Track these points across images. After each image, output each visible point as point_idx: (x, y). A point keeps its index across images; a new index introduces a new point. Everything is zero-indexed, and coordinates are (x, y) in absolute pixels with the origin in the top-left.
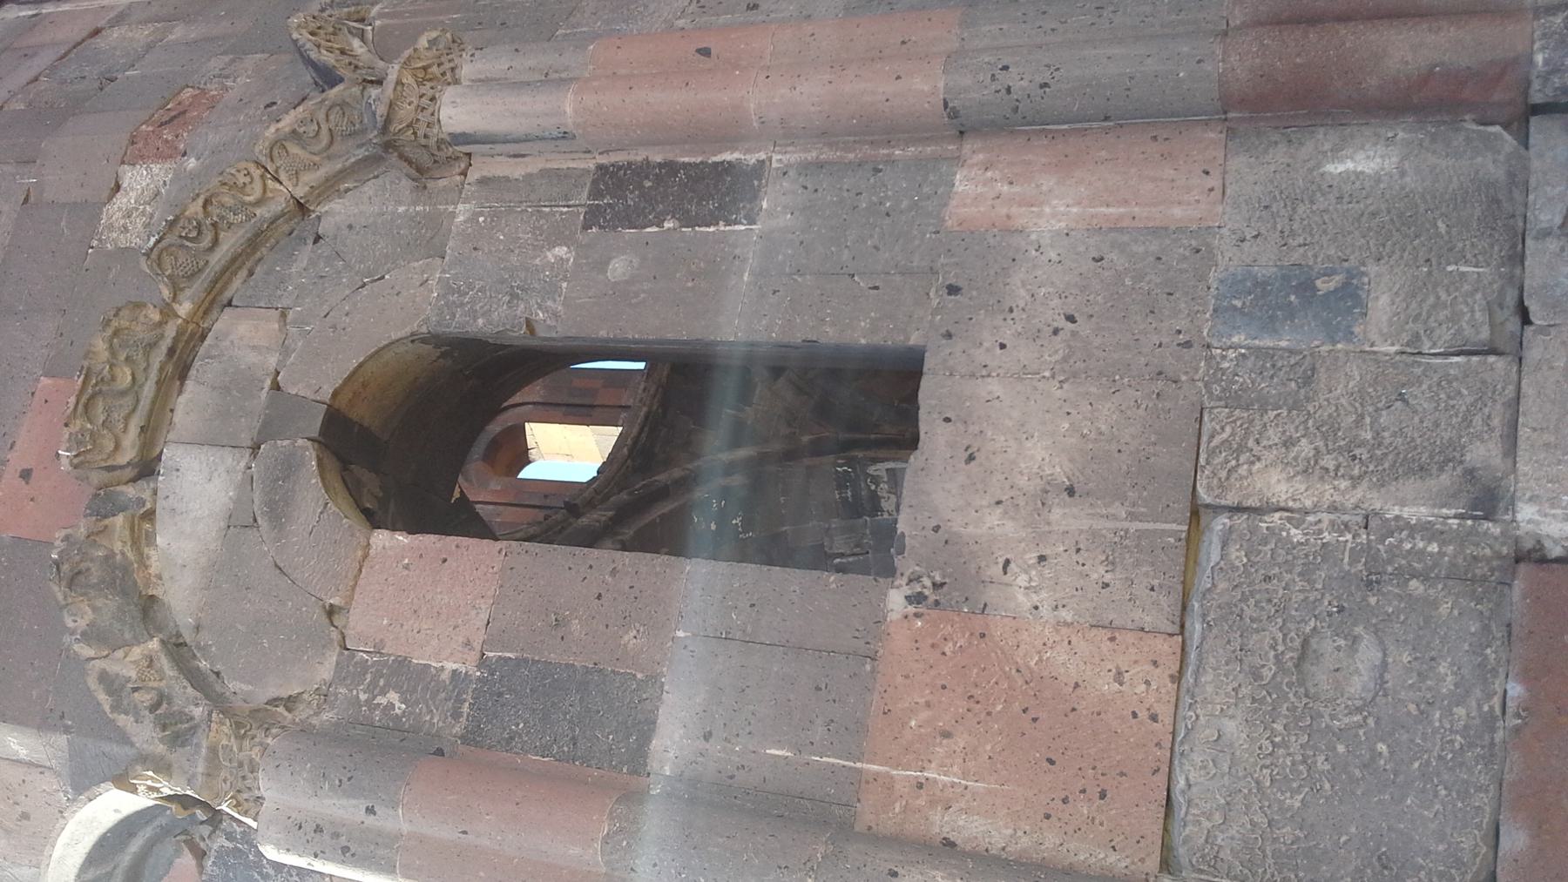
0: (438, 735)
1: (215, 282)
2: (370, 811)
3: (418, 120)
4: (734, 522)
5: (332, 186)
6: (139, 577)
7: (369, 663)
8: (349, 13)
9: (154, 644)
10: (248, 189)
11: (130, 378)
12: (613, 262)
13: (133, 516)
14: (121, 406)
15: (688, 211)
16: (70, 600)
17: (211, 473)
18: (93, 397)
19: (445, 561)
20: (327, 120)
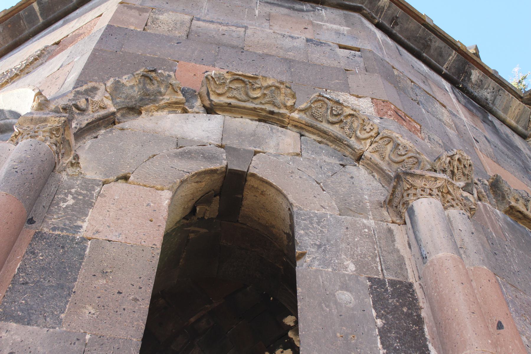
1: (312, 126)
3: (416, 189)
5: (374, 169)
6: (151, 106)
7: (93, 192)
8: (481, 192)
9: (113, 109)
10: (363, 132)
11: (255, 96)
12: (349, 293)
13: (183, 104)
14: (240, 94)
15: (390, 332)
16: (136, 76)
17: (207, 131)
18: (244, 82)
19: (151, 221)
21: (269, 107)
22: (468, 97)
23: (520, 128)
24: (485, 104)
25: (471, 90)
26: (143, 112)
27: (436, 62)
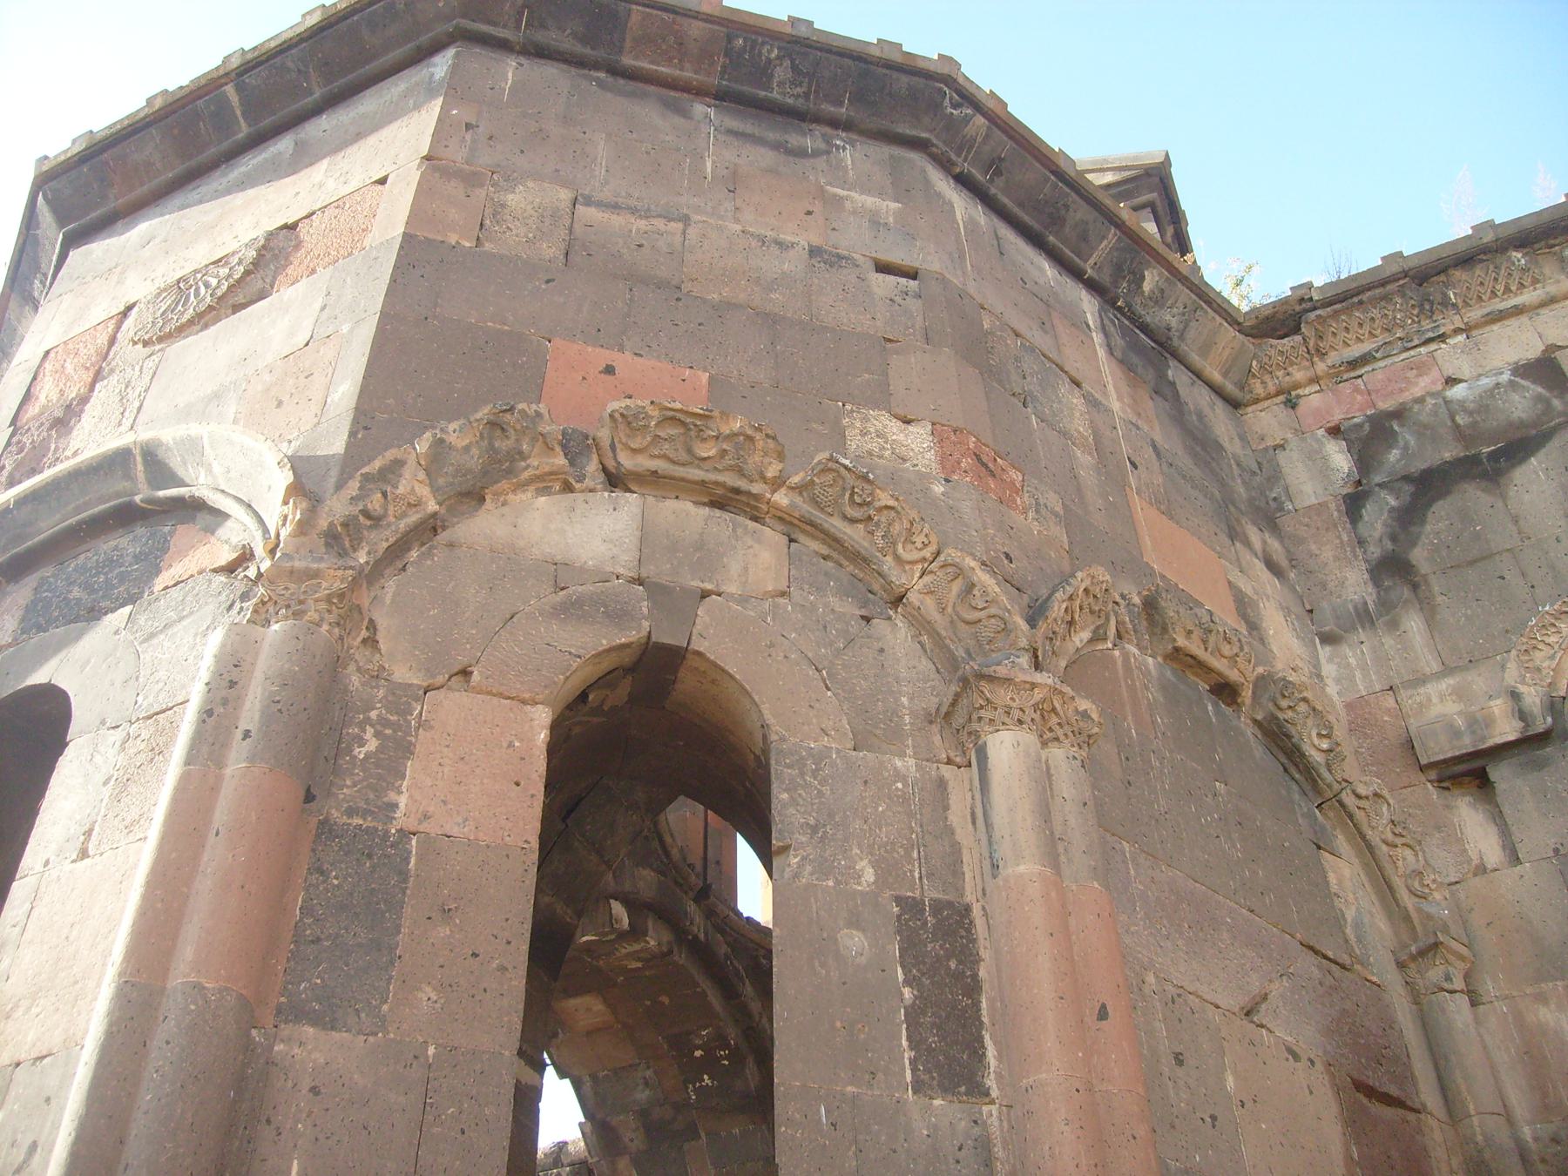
0: (329, 794)
1: (812, 524)
2: (247, 734)
3: (996, 709)
4: (706, 1077)
5: (924, 628)
6: (504, 484)
7: (409, 717)
9: (432, 506)
10: (909, 546)
11: (706, 455)
12: (860, 934)
13: (565, 473)
14: (676, 450)
15: (924, 1013)
16: (475, 425)
17: (611, 541)
18: (683, 424)
19: (518, 784)
20: (990, 617)
21: (731, 480)
22: (1131, 326)
23: (1230, 388)
24: (1164, 340)
25: (1139, 310)
26: (488, 498)
27: (1072, 252)
